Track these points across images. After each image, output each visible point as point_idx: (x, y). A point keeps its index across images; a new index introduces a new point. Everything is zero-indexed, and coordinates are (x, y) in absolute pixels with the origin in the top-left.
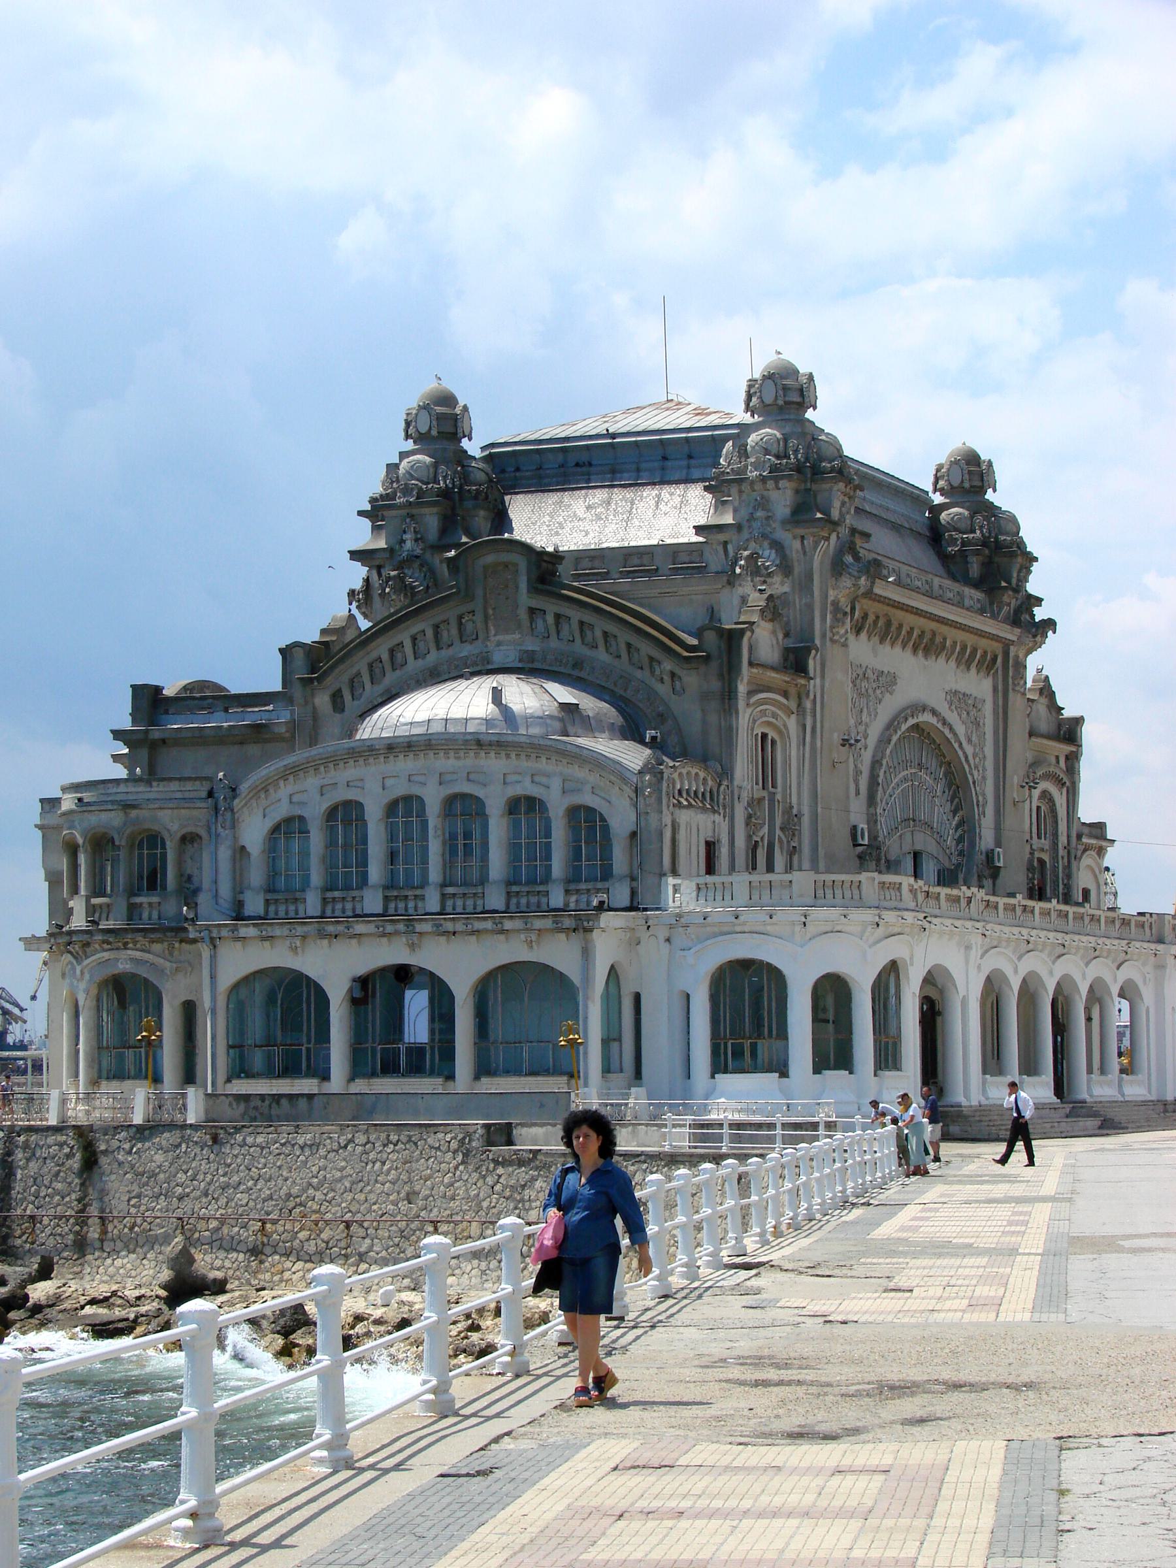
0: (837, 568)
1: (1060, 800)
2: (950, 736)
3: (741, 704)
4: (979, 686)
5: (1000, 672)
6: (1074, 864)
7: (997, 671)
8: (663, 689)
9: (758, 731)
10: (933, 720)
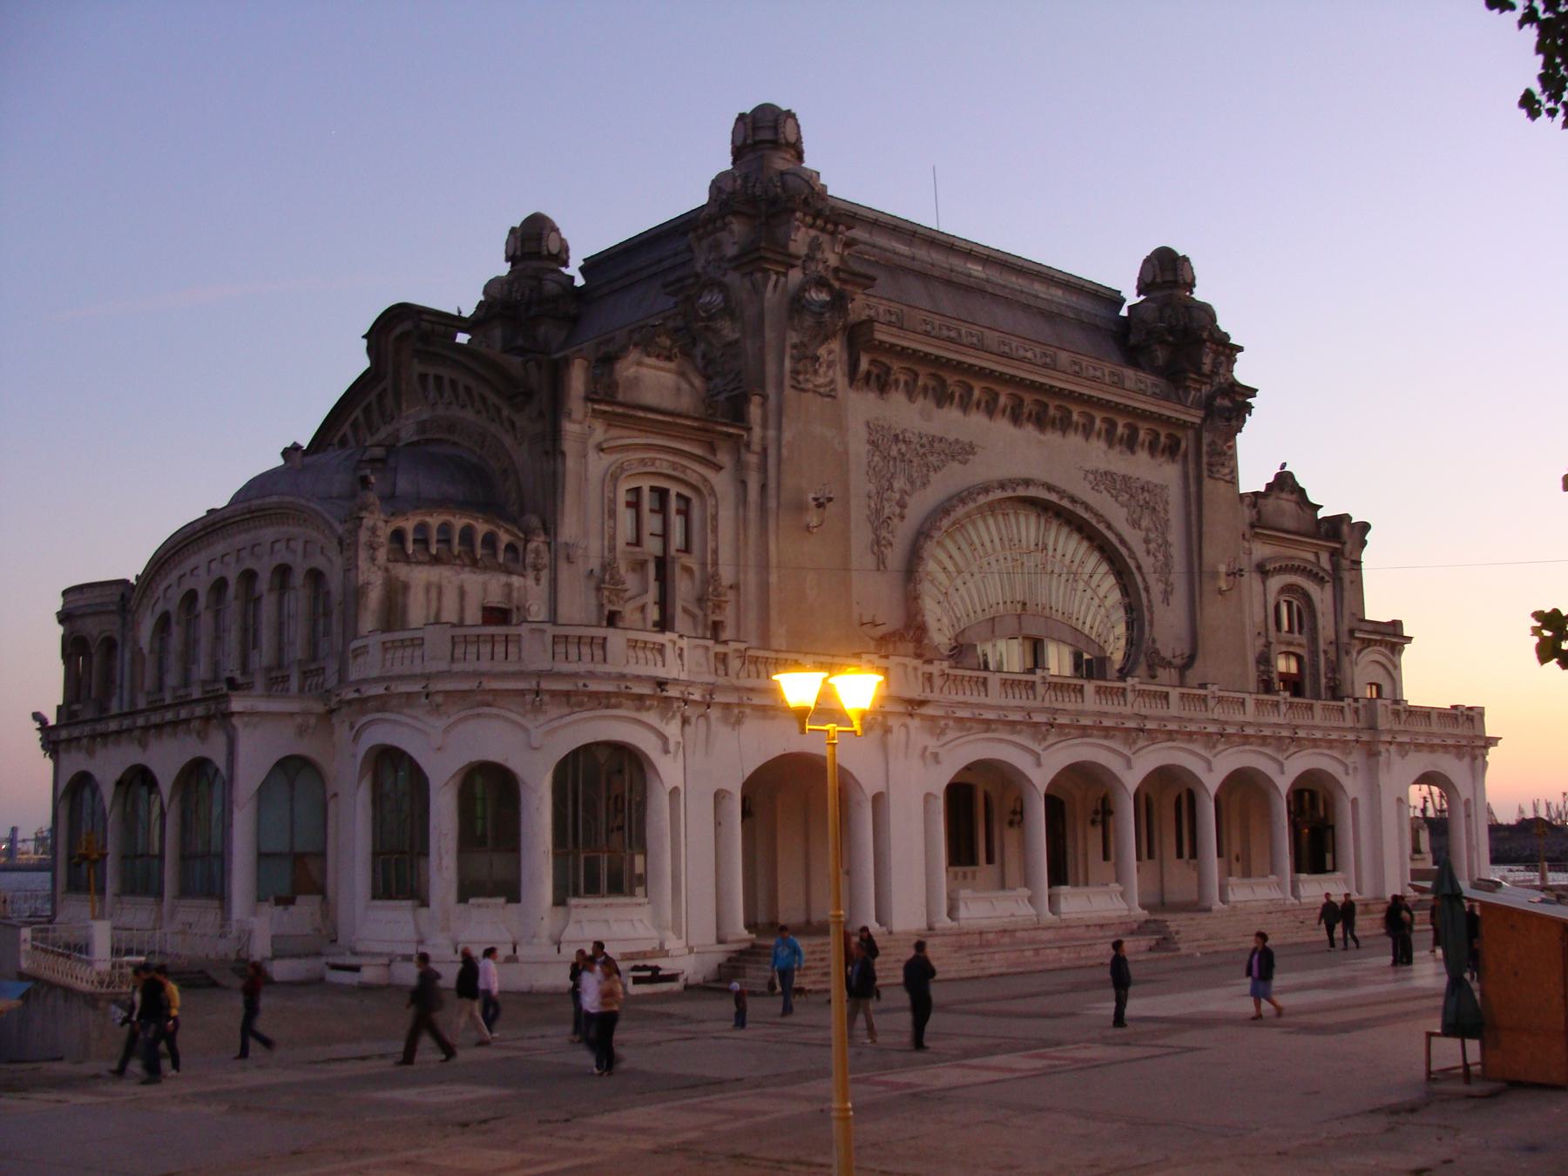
0: (797, 304)
1: (1322, 597)
2: (1086, 516)
3: (569, 446)
4: (1166, 475)
5: (1191, 457)
6: (1345, 661)
7: (1185, 456)
8: (508, 441)
9: (645, 484)
10: (1053, 497)
